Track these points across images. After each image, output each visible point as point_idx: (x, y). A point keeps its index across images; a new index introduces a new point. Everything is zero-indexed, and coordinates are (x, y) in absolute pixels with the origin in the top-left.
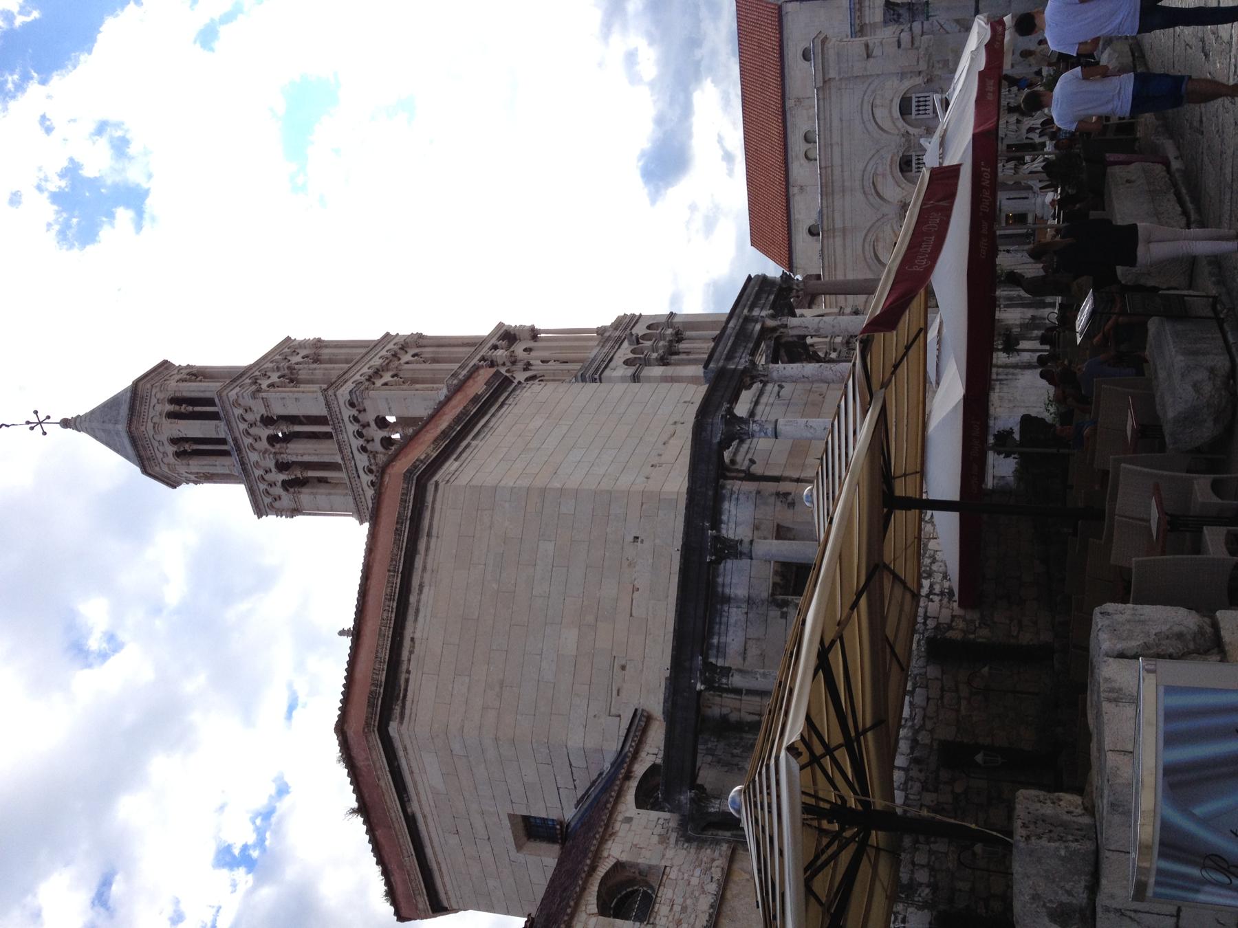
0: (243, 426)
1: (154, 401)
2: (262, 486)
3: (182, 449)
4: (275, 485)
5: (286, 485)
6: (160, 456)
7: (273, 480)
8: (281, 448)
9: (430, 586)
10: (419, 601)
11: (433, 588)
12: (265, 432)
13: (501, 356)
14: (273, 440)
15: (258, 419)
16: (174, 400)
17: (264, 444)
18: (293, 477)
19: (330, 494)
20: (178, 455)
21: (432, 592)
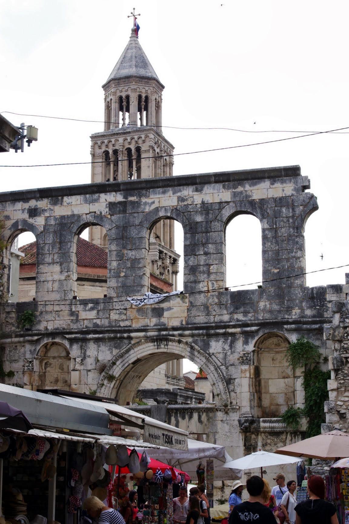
0: (136, 137)
1: (147, 88)
2: (106, 141)
3: (124, 101)
4: (106, 148)
5: (106, 153)
6: (120, 89)
7: (109, 147)
8: (125, 154)
9: (102, 290)
10: (97, 286)
11: (101, 291)
12: (133, 147)
13: (167, 263)
14: (129, 150)
15: (139, 145)
16: (147, 98)
17: (127, 146)
18: (111, 157)
19: (102, 175)
20: (121, 98)
21: (100, 291)
